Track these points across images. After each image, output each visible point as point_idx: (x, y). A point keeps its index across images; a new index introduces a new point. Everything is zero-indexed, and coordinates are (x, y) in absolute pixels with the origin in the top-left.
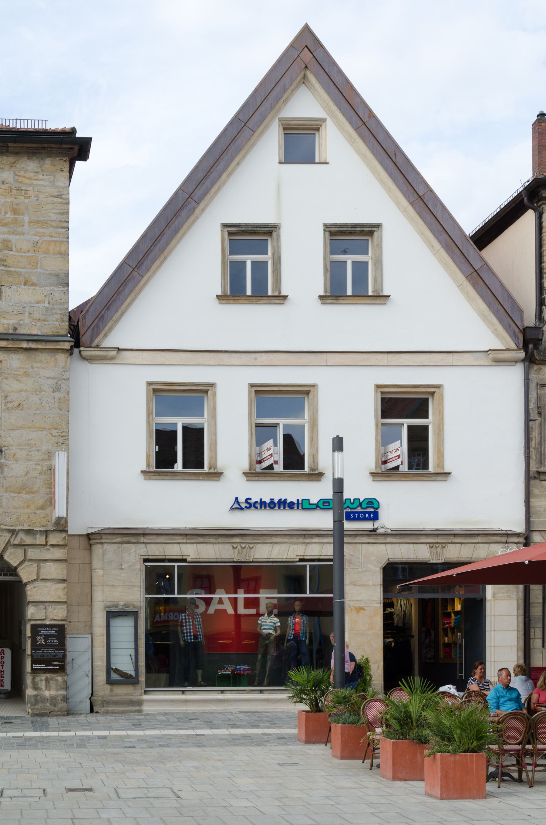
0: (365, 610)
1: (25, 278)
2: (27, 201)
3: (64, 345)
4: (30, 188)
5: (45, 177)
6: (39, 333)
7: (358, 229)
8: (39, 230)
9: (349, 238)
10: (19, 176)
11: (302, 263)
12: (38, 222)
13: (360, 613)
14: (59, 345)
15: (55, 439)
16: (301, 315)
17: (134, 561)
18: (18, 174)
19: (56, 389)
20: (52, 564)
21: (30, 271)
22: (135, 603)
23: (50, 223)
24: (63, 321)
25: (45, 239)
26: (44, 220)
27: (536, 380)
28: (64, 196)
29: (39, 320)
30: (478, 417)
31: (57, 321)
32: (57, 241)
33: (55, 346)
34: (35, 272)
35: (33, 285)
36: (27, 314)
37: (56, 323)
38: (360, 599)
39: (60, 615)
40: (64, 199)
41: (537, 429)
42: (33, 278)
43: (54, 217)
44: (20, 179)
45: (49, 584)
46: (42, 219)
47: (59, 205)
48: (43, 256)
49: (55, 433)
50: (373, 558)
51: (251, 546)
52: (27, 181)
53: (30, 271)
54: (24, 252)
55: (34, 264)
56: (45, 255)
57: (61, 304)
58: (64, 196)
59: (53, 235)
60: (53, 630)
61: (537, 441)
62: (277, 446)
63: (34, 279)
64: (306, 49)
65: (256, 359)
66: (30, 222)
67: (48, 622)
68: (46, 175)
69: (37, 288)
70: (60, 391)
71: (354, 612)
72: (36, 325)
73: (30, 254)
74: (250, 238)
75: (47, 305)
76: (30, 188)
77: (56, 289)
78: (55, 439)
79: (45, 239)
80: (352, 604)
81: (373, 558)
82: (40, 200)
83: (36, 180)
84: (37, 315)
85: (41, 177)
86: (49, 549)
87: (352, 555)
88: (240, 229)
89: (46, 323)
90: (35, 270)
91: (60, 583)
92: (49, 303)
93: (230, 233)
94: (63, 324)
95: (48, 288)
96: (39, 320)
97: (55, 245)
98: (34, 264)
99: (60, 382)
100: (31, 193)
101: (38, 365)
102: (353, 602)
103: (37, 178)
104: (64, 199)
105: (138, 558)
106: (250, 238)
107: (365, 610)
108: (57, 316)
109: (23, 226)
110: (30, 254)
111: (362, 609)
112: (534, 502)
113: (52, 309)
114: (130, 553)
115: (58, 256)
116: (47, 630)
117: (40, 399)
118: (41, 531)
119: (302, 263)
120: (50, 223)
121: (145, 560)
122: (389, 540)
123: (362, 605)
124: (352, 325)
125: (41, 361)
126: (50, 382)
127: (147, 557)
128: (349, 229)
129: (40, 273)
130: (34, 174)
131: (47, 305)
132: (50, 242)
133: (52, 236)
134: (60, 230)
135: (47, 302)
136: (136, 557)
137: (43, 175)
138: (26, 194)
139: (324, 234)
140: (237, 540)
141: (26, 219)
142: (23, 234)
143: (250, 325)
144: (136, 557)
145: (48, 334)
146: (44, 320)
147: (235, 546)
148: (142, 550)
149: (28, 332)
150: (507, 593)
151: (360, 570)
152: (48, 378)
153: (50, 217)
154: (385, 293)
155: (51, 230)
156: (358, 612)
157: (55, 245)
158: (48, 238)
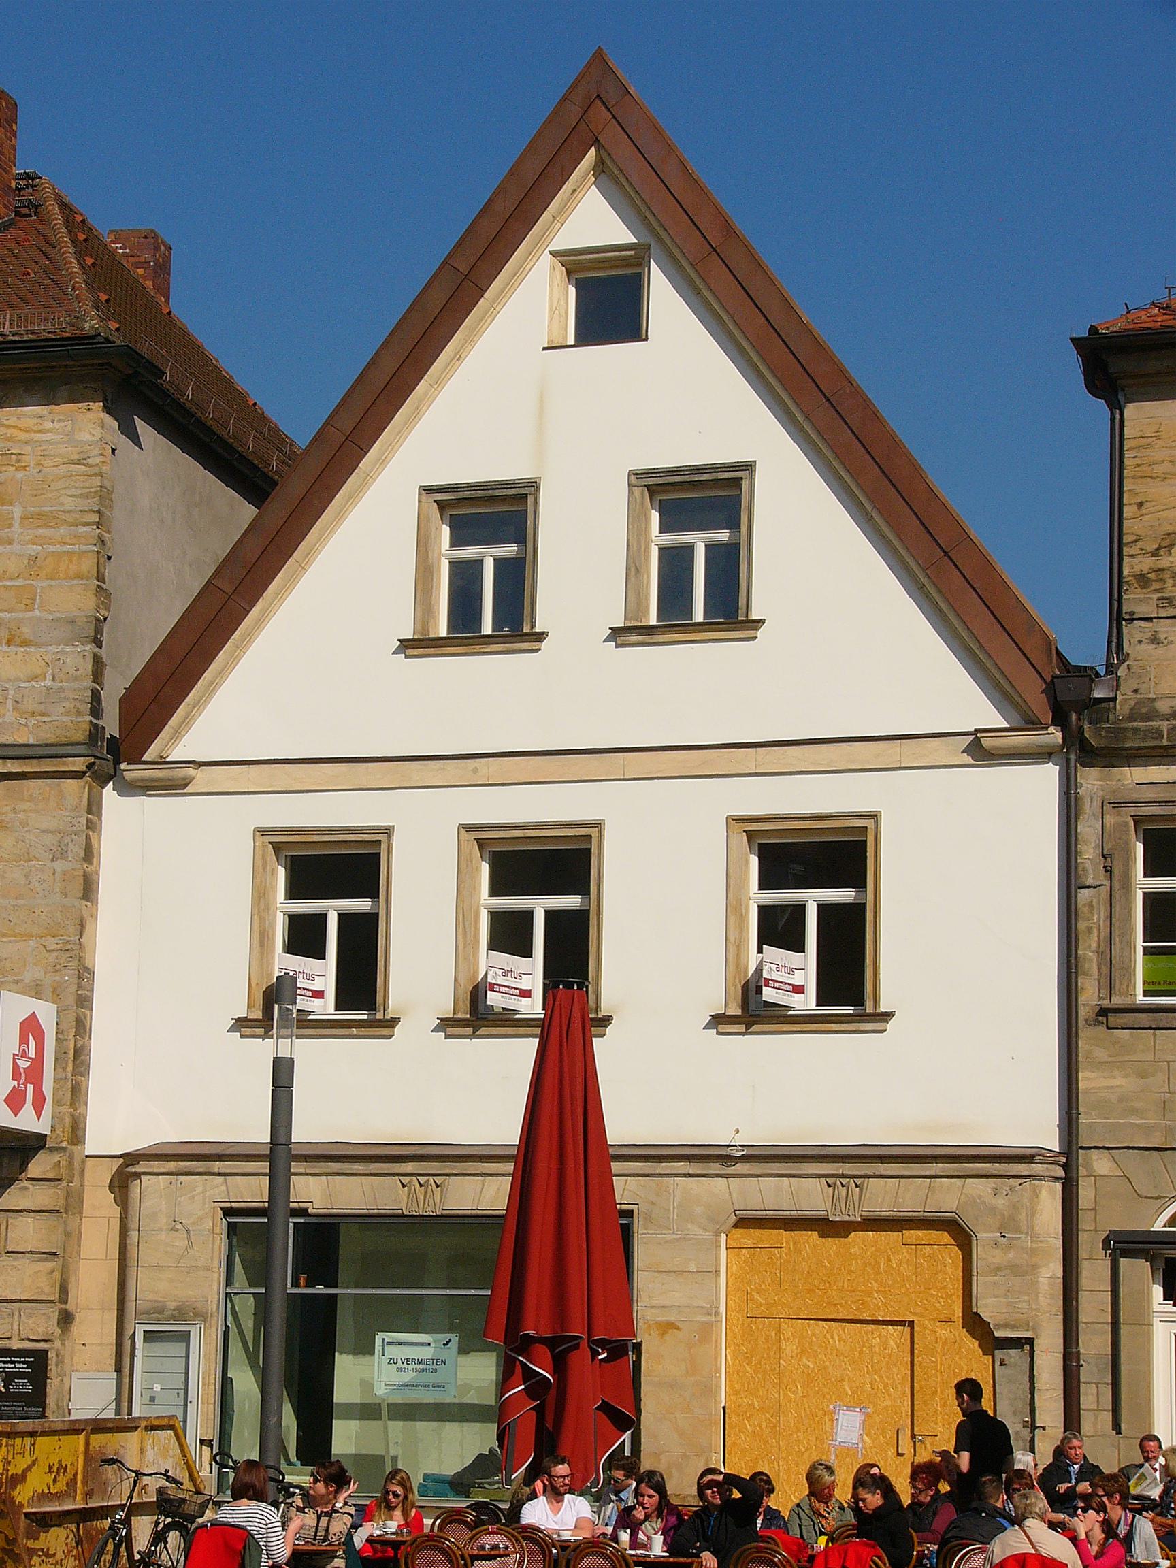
0: (678, 1329)
1: (10, 630)
2: (19, 475)
3: (74, 764)
4: (27, 449)
5: (56, 425)
6: (31, 741)
7: (705, 477)
8: (41, 531)
9: (701, 500)
10: (8, 427)
11: (586, 558)
12: (39, 516)
13: (667, 1337)
14: (65, 764)
15: (52, 958)
16: (583, 674)
17: (200, 1213)
18: (6, 422)
19: (58, 854)
20: (29, 1220)
21: (20, 615)
22: (198, 1305)
23: (62, 516)
24: (79, 713)
25: (51, 548)
26: (51, 512)
27: (1101, 793)
28: (90, 461)
29: (33, 714)
30: (980, 870)
31: (67, 713)
32: (74, 552)
33: (55, 765)
34: (31, 618)
35: (26, 643)
36: (9, 702)
37: (65, 719)
38: (668, 1303)
39: (40, 1330)
40: (90, 466)
41: (1102, 908)
42: (25, 630)
43: (70, 503)
44: (10, 432)
45: (23, 1261)
46: (46, 509)
47: (81, 478)
48: (44, 584)
49: (51, 943)
50: (699, 1210)
51: (439, 1180)
52: (22, 436)
53: (20, 615)
54: (11, 579)
55: (28, 602)
56: (50, 582)
57: (76, 678)
58: (90, 461)
59: (68, 540)
60: (24, 1363)
61: (1102, 935)
62: (277, 1061)
63: (26, 630)
64: (598, 102)
65: (475, 770)
66: (24, 518)
67: (15, 1345)
68: (59, 421)
69: (32, 649)
70: (65, 858)
71: (655, 1333)
72: (26, 725)
73: (20, 582)
74: (492, 515)
75: (48, 683)
76: (27, 449)
77: (68, 648)
78: (52, 958)
79: (51, 548)
80: (650, 1315)
81: (699, 1210)
82: (45, 470)
83: (40, 432)
84: (29, 704)
85: (48, 425)
86: (26, 1188)
87: (653, 1203)
88: (460, 495)
89: (46, 719)
90: (31, 614)
91: (46, 1260)
92: (53, 680)
93: (442, 506)
94: (80, 719)
95: (54, 649)
96: (33, 714)
97: (71, 561)
98: (28, 602)
99: (68, 839)
100: (29, 460)
101: (26, 806)
102: (653, 1311)
103: (40, 428)
104: (90, 466)
105: (209, 1206)
106: (492, 515)
107: (678, 1329)
108: (67, 704)
109: (11, 526)
110: (20, 582)
111: (672, 1326)
112: (1087, 1079)
113: (61, 689)
114: (193, 1197)
115: (76, 582)
116: (11, 1362)
117: (26, 876)
118: (12, 1149)
119: (586, 558)
120: (62, 516)
121: (227, 1212)
122: (740, 1168)
123: (672, 1318)
124: (696, 685)
125: (31, 798)
126: (48, 839)
127: (228, 1205)
128: (687, 478)
129: (40, 618)
130: (35, 421)
131: (48, 683)
132: (59, 555)
133: (65, 543)
134: (81, 529)
135: (49, 677)
136: (204, 1204)
137: (53, 422)
138: (18, 461)
139: (631, 493)
140: (409, 1167)
141: (17, 511)
142: (10, 542)
143: (484, 696)
144: (204, 1204)
145: (49, 742)
146: (43, 714)
147: (405, 1180)
148: (217, 1190)
149: (11, 740)
150: (1006, 1296)
151: (669, 1237)
152: (43, 831)
153: (63, 504)
154: (754, 616)
155: (63, 530)
156: (663, 1333)
157: (71, 561)
158: (58, 548)
